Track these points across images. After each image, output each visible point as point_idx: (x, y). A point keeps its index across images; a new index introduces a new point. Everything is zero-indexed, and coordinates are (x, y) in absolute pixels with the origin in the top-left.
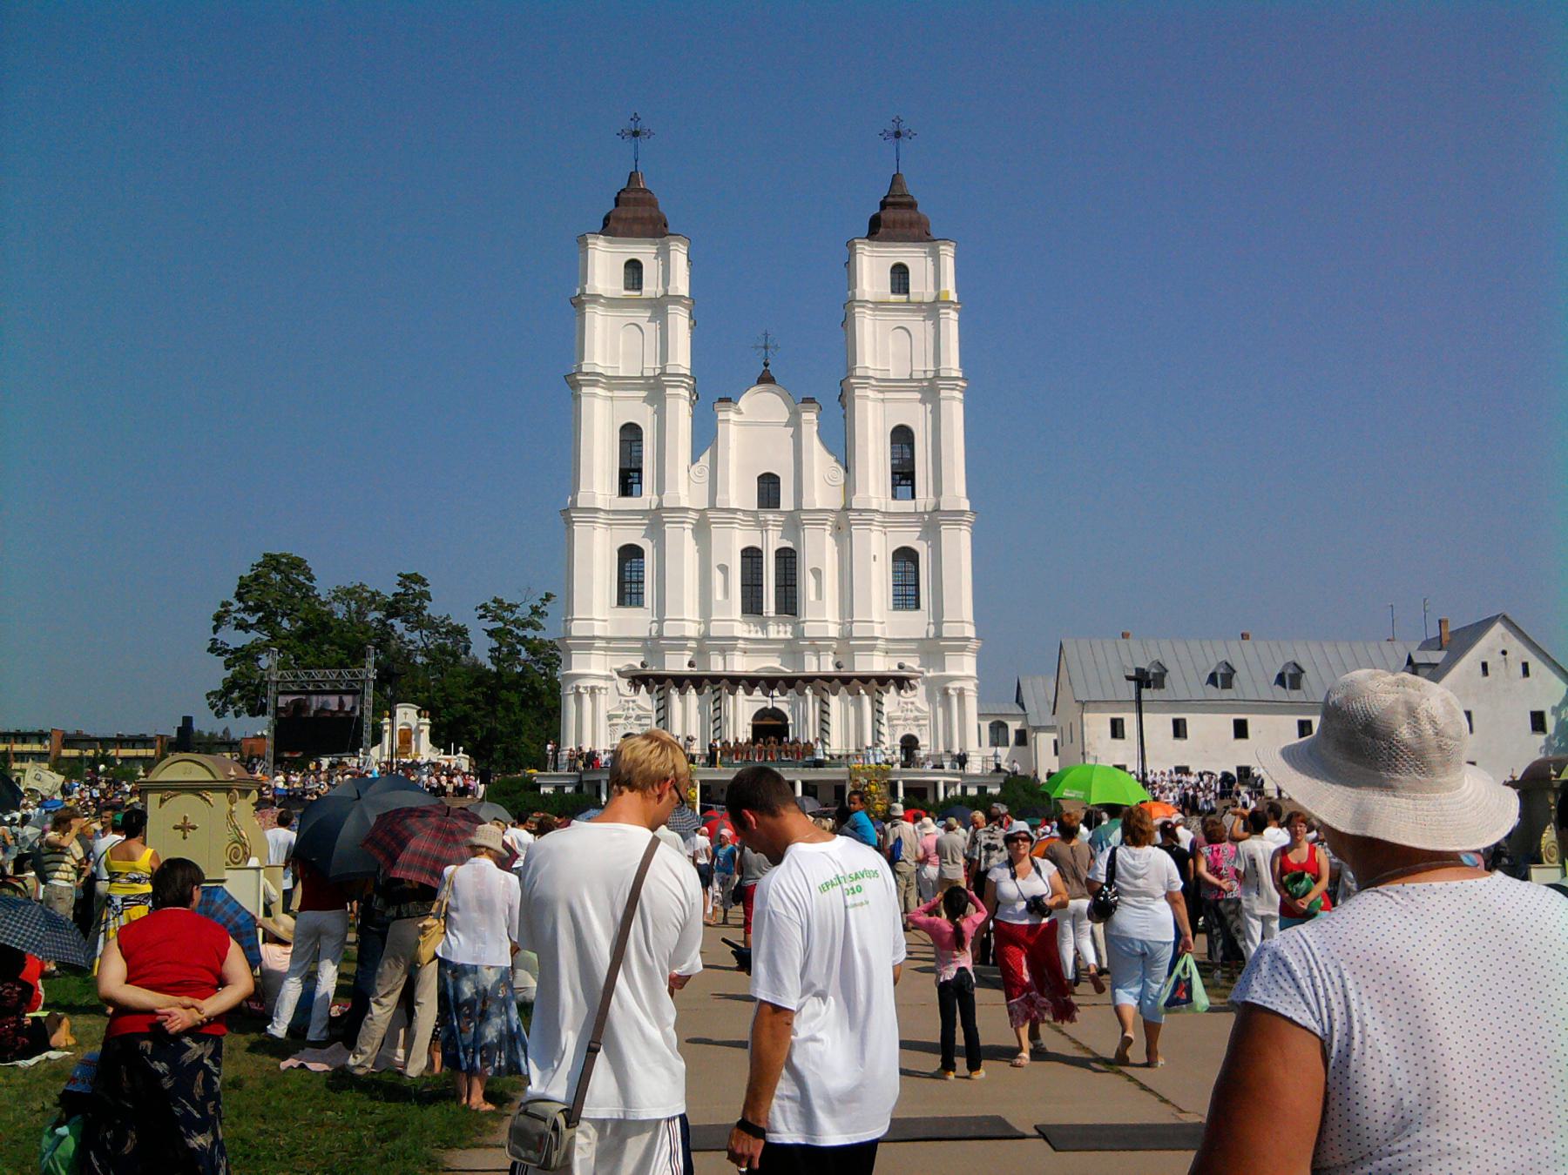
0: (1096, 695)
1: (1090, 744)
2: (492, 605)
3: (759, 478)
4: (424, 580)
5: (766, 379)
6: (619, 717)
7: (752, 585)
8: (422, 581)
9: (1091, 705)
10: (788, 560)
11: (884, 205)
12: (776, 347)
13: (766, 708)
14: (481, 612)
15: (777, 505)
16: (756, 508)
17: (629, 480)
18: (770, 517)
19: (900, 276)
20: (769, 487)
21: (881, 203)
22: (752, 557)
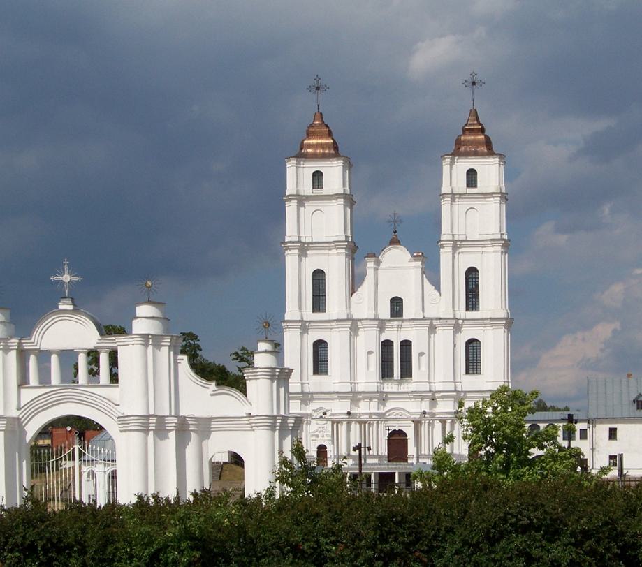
0: (602, 415)
1: (596, 443)
2: (240, 353)
3: (391, 300)
4: (197, 336)
5: (395, 242)
6: (317, 436)
7: (387, 362)
8: (195, 338)
9: (598, 420)
10: (406, 345)
11: (465, 131)
12: (401, 221)
13: (395, 430)
14: (234, 356)
15: (401, 315)
16: (389, 318)
17: (319, 302)
18: (396, 323)
19: (472, 176)
20: (396, 306)
21: (456, 140)
22: (387, 346)
